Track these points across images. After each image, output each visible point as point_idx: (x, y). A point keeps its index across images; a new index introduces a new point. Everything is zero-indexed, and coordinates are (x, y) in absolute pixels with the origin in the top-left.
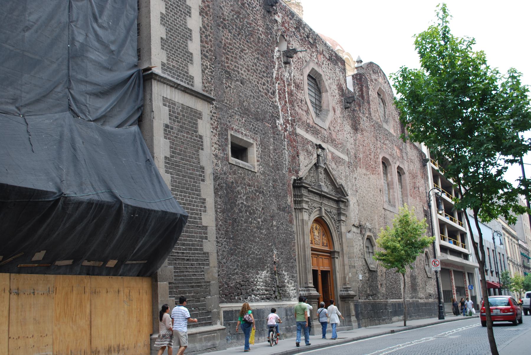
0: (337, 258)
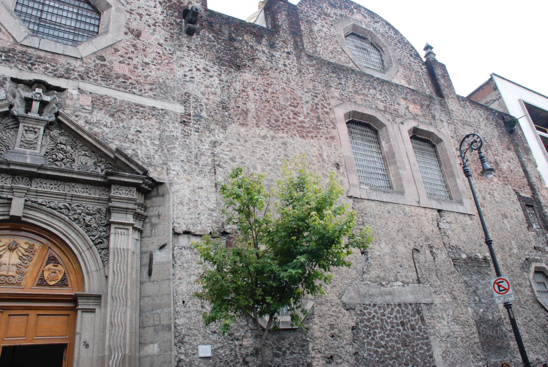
0: (93, 311)
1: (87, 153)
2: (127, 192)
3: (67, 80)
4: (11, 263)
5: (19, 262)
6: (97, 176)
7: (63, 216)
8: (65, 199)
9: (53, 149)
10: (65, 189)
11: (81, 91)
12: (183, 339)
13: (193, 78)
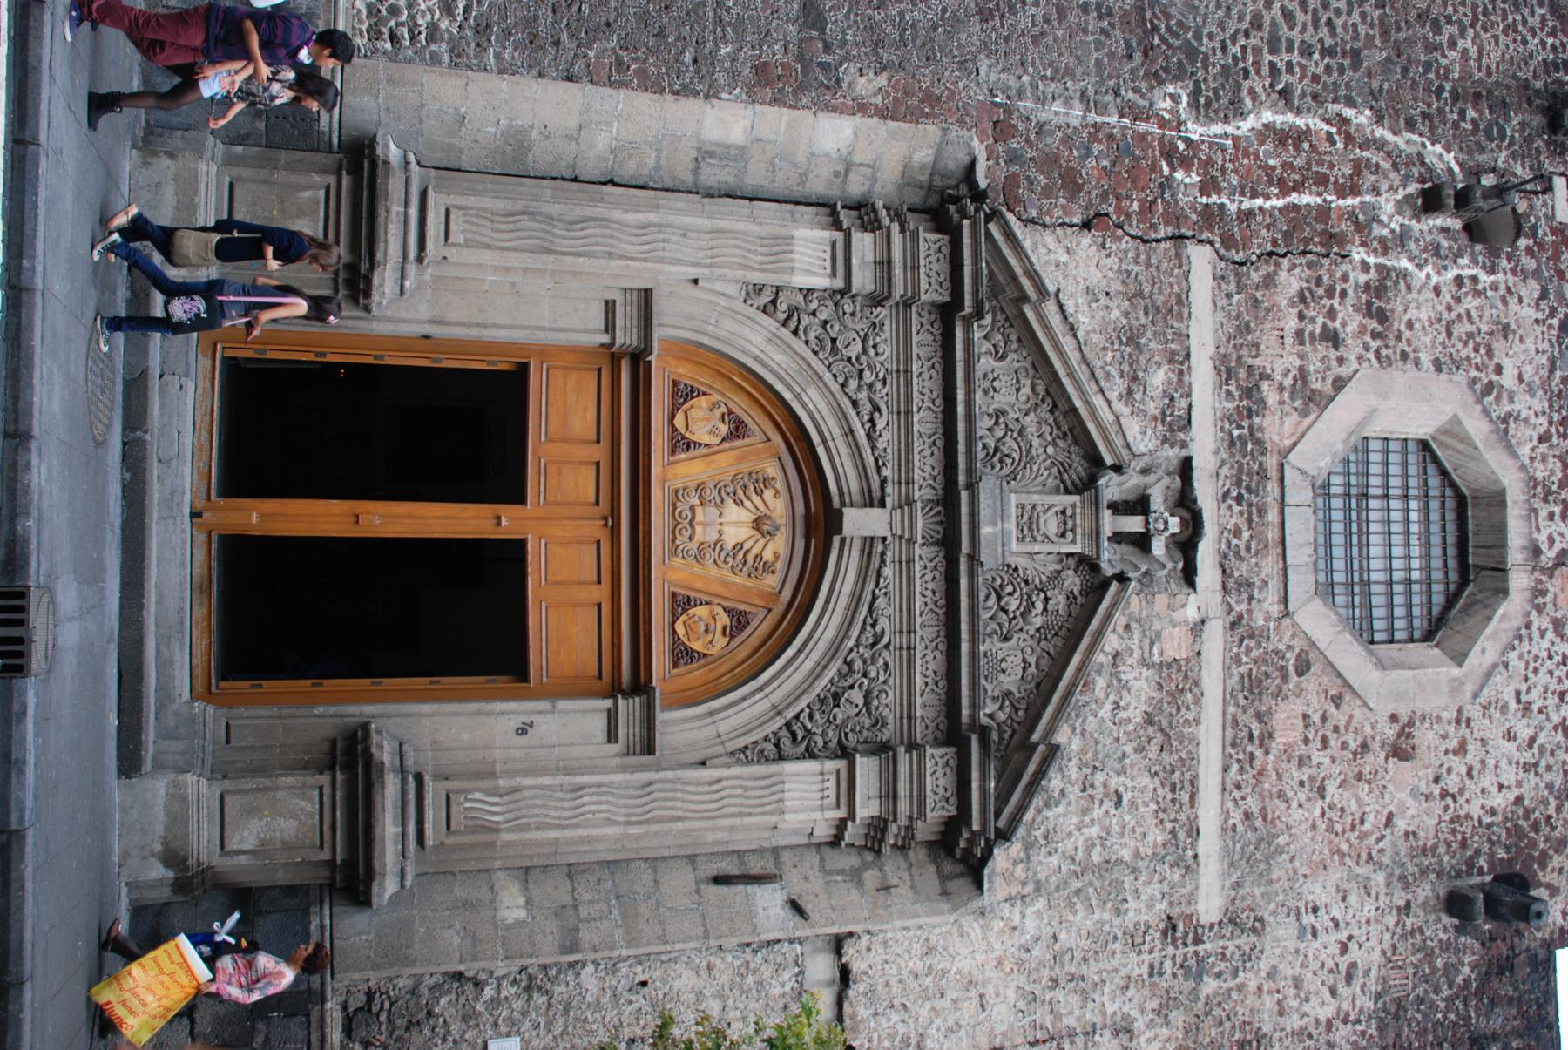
0: (612, 737)
1: (1032, 669)
2: (941, 791)
3: (1218, 587)
4: (725, 529)
5: (729, 546)
6: (974, 706)
7: (855, 633)
8: (901, 632)
9: (1026, 582)
10: (927, 630)
11: (1198, 627)
12: (539, 988)
13: (1314, 935)
